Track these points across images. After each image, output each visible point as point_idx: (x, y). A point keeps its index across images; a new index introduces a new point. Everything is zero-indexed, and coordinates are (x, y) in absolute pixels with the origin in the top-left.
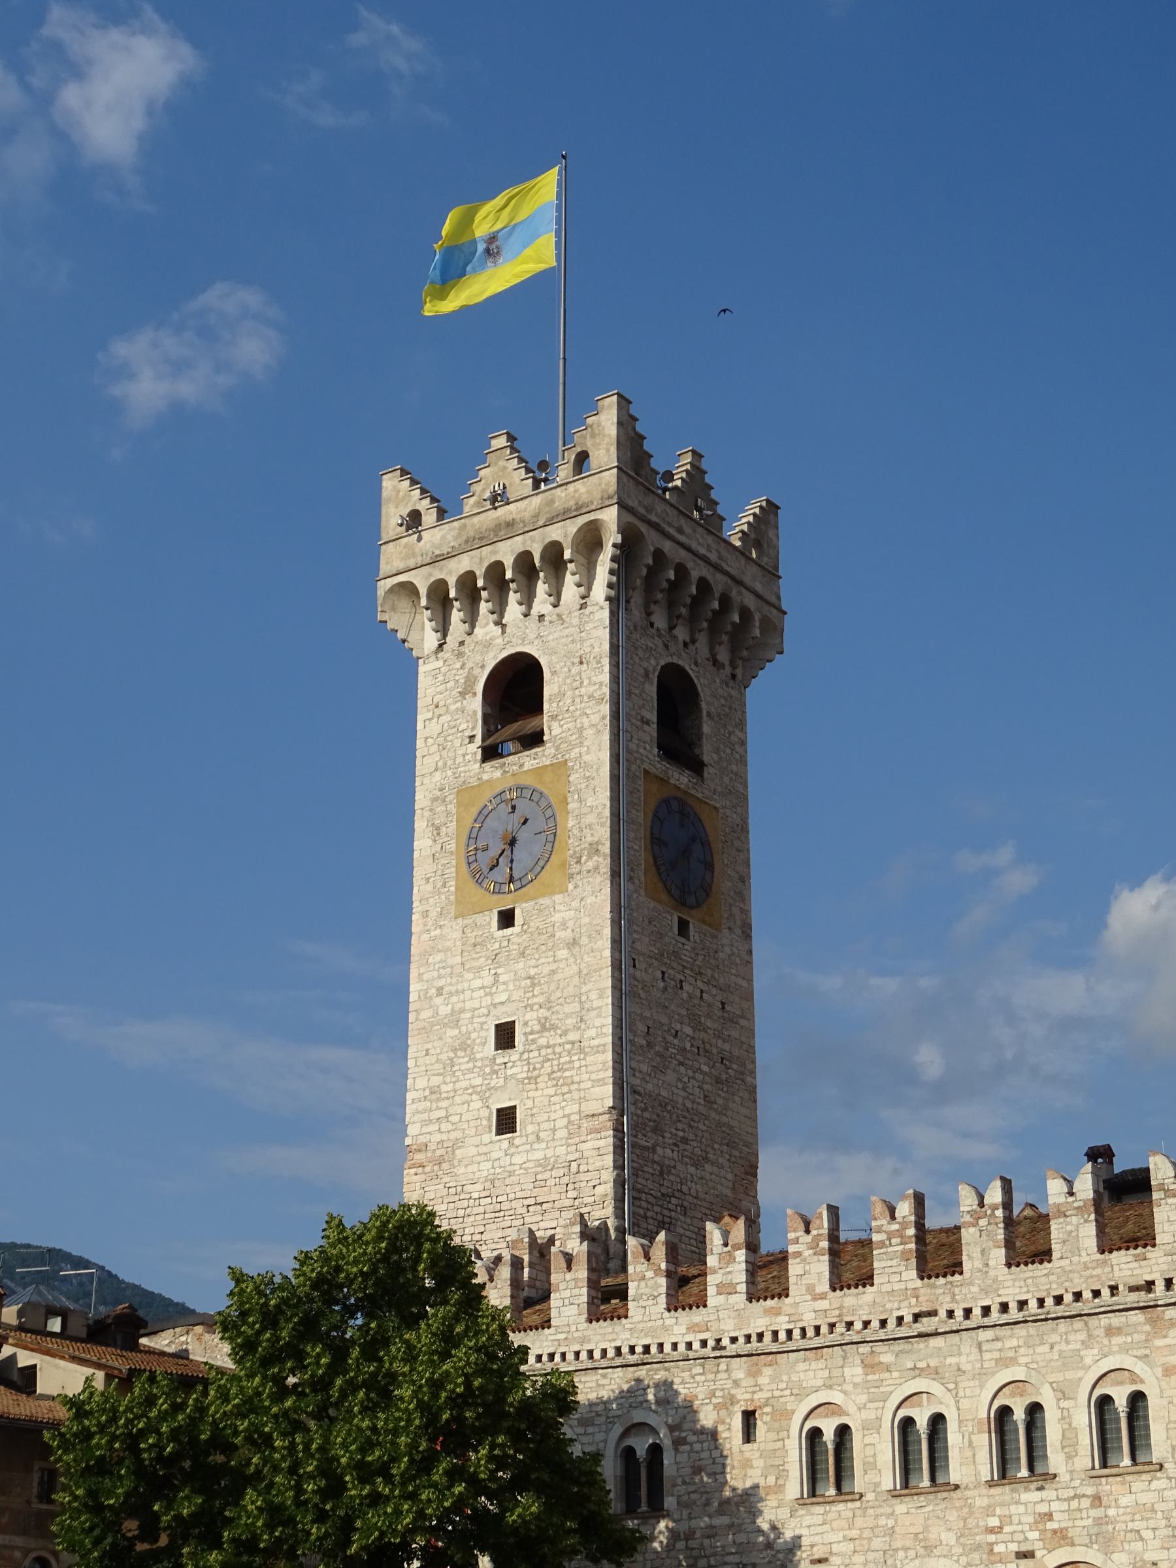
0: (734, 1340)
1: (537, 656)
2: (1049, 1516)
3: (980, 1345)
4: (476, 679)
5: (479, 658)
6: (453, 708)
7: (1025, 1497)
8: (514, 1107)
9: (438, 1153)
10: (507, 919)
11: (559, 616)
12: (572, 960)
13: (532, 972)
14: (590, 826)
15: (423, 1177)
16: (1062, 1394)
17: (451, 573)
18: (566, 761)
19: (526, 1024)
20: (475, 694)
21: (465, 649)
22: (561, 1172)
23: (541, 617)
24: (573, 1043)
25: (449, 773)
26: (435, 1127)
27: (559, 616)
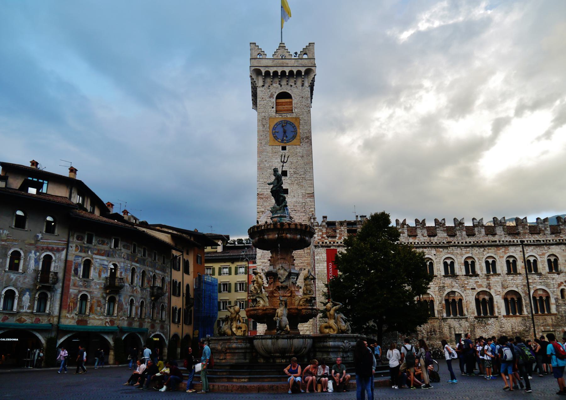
0: (405, 243)
1: (290, 93)
2: (478, 282)
3: (461, 249)
4: (274, 95)
5: (274, 90)
6: (267, 100)
7: (473, 278)
8: (288, 189)
9: (267, 196)
10: (284, 148)
11: (296, 87)
12: (302, 160)
13: (292, 161)
14: (306, 133)
15: (263, 201)
16: (479, 259)
17: (272, 70)
18: (299, 118)
19: (290, 172)
20: (273, 98)
21: (271, 87)
22: (301, 204)
23: (291, 86)
24: (303, 178)
25: (267, 114)
26: (266, 190)
27: (296, 87)
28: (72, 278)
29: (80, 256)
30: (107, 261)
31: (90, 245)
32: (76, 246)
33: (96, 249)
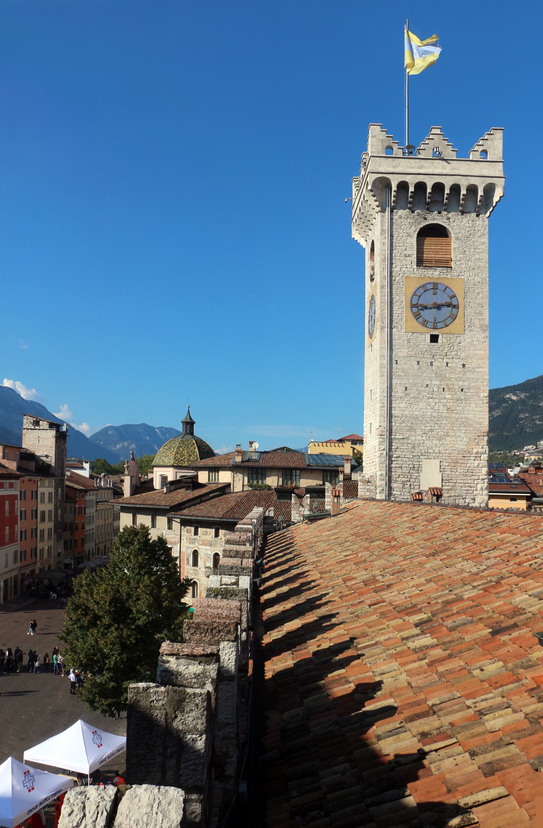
28: (186, 567)
29: (190, 548)
30: (210, 550)
31: (196, 537)
32: (187, 538)
33: (201, 540)
